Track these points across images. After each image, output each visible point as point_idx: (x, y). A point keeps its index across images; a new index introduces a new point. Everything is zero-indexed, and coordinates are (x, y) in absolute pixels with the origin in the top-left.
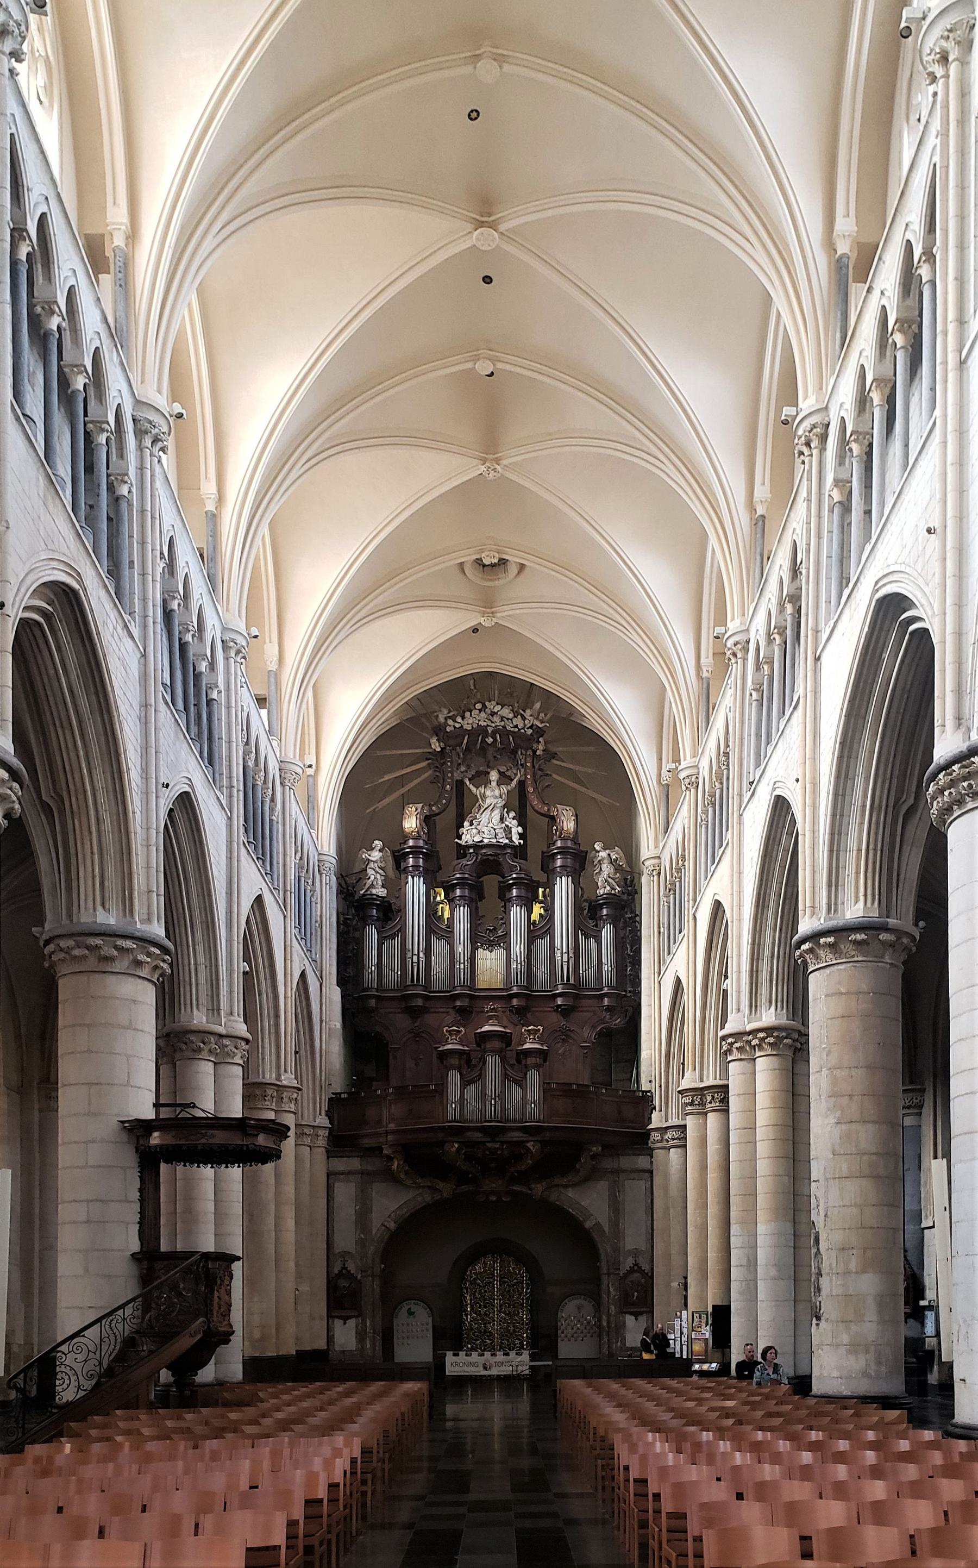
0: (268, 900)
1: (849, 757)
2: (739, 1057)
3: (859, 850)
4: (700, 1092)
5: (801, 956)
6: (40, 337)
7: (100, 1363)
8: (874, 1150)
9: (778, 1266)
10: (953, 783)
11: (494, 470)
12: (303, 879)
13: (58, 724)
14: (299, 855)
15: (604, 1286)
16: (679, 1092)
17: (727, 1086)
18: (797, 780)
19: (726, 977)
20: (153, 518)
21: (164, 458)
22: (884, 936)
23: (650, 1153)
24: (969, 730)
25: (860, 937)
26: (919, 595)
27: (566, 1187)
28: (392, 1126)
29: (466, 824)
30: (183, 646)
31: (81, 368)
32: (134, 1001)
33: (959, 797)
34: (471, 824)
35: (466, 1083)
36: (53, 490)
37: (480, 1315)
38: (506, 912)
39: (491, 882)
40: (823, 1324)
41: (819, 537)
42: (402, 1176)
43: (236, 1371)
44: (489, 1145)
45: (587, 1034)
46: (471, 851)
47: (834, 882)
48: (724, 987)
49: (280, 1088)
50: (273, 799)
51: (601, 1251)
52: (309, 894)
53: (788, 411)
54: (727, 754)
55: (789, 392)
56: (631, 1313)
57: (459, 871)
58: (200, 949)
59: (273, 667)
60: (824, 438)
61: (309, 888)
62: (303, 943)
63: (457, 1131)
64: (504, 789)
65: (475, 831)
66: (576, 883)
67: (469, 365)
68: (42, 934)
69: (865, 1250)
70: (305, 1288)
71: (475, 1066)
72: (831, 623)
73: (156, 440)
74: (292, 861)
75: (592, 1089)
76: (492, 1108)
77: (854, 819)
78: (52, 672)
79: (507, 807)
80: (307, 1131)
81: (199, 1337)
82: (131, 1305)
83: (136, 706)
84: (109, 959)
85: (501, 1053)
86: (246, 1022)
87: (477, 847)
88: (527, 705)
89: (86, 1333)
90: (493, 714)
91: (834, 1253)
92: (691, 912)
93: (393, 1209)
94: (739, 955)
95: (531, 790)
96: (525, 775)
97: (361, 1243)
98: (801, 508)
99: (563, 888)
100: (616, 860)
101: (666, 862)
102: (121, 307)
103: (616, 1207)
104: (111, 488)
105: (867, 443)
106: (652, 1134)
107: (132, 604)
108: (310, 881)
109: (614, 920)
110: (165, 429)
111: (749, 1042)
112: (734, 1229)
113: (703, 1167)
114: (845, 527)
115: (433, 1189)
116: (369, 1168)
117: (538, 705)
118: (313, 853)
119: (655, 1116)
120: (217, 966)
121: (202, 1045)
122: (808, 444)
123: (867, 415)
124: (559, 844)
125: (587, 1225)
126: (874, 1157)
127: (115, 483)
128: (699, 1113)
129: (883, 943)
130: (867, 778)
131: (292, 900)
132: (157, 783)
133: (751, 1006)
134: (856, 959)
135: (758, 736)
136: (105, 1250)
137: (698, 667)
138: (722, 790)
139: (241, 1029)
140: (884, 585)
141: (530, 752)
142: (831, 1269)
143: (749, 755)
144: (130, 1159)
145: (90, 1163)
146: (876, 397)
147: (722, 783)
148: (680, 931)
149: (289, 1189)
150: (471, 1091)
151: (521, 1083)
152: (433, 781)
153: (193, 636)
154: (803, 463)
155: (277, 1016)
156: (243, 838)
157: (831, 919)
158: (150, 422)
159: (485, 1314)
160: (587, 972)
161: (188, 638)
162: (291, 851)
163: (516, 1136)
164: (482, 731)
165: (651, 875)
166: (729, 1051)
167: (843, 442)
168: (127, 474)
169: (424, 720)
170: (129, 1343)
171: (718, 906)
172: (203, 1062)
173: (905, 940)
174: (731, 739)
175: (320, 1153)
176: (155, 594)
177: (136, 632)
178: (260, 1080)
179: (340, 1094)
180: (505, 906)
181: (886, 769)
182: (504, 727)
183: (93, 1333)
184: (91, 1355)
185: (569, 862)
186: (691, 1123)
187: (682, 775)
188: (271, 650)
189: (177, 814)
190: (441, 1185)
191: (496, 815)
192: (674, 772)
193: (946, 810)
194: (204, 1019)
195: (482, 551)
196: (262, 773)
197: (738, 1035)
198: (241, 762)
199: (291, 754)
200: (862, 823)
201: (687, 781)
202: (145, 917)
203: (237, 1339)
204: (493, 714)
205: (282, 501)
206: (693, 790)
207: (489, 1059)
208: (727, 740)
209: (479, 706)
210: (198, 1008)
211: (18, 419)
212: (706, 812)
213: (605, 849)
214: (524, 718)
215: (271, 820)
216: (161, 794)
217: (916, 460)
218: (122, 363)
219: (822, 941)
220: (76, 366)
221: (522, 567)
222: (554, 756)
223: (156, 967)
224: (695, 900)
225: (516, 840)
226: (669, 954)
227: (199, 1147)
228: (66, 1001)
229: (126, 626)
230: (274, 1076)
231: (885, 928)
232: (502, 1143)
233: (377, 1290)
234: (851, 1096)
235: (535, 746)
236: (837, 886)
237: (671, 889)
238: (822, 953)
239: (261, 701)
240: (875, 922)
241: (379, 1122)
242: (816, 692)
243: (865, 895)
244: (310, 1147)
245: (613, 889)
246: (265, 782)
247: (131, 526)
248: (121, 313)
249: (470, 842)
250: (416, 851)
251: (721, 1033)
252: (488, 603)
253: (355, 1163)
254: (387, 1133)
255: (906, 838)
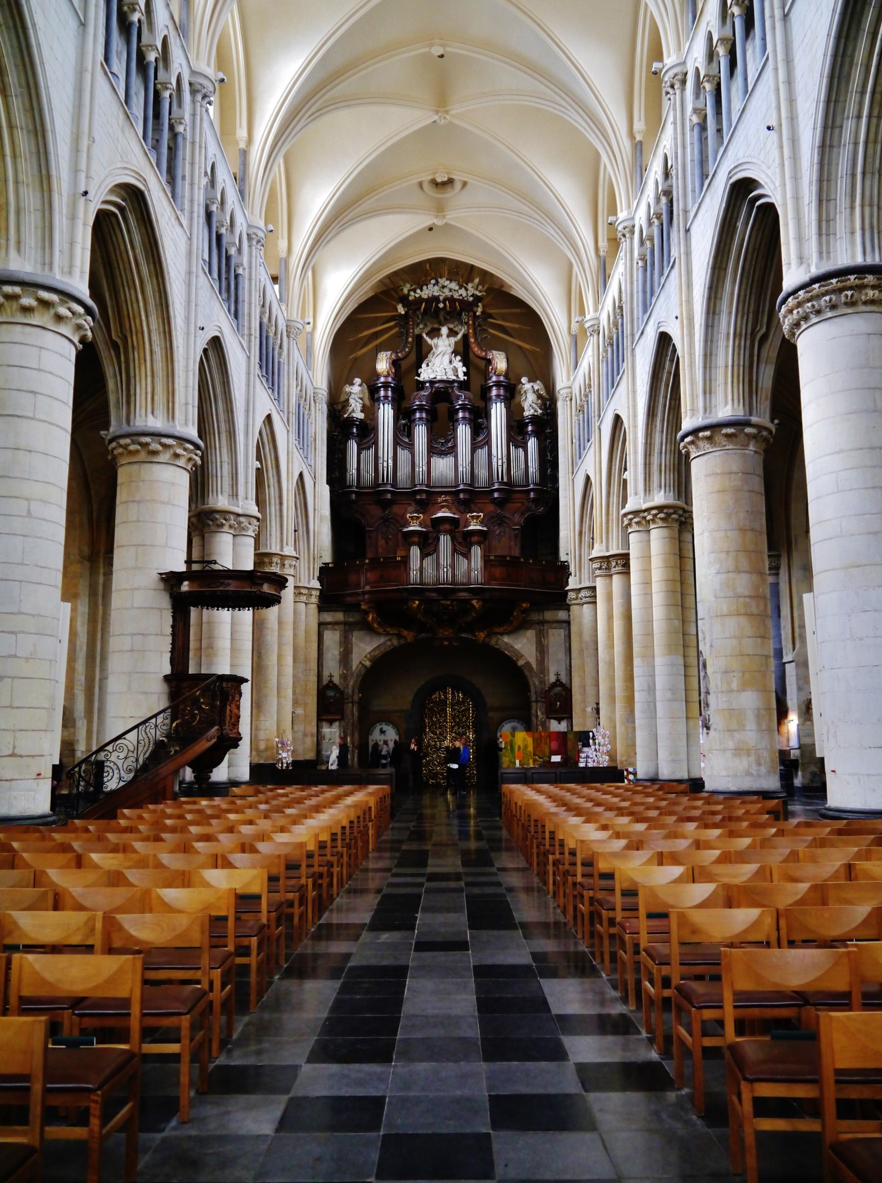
0: (276, 418)
1: (715, 298)
2: (637, 529)
3: (727, 366)
4: (607, 559)
5: (685, 447)
6: (125, 26)
7: (137, 760)
8: (747, 593)
9: (673, 690)
10: (799, 305)
11: (445, 118)
12: (302, 406)
13: (125, 284)
14: (299, 388)
15: (533, 711)
16: (590, 560)
17: (628, 555)
18: (677, 318)
19: (625, 469)
20: (200, 147)
21: (211, 109)
22: (748, 430)
23: (567, 608)
24: (809, 266)
25: (730, 430)
26: (763, 176)
27: (502, 634)
28: (367, 588)
29: (424, 365)
30: (219, 237)
31: (153, 47)
32: (173, 484)
33: (804, 315)
34: (428, 365)
35: (423, 556)
36: (129, 123)
37: (436, 734)
38: (455, 430)
39: (442, 407)
40: (711, 732)
41: (684, 147)
42: (376, 626)
43: (244, 774)
44: (443, 602)
45: (518, 520)
46: (428, 385)
47: (708, 391)
48: (625, 477)
49: (283, 557)
50: (281, 347)
51: (531, 683)
52: (306, 417)
53: (656, 66)
54: (621, 308)
55: (657, 53)
56: (555, 719)
57: (420, 399)
58: (225, 451)
59: (283, 254)
60: (684, 82)
61: (306, 412)
62: (301, 451)
63: (419, 592)
64: (453, 340)
65: (430, 371)
66: (508, 408)
67: (427, 50)
68: (106, 435)
69: (744, 673)
70: (300, 711)
71: (431, 544)
72: (697, 205)
73: (205, 96)
74: (294, 392)
75: (522, 560)
76: (445, 574)
77: (722, 343)
78: (122, 248)
79: (455, 352)
80: (304, 591)
81: (214, 740)
82: (161, 715)
83: (183, 273)
84: (155, 453)
85: (452, 533)
86: (258, 504)
87: (432, 382)
88: (469, 280)
89: (127, 736)
90: (443, 287)
91: (719, 676)
92: (597, 424)
93: (368, 651)
94: (636, 453)
95: (472, 340)
96: (468, 330)
97: (344, 677)
98: (669, 129)
99: (498, 413)
100: (538, 391)
101: (576, 391)
102: (184, 13)
103: (542, 650)
104: (172, 128)
105: (715, 82)
106: (569, 593)
107: (183, 203)
108: (307, 408)
109: (537, 434)
110: (211, 89)
111: (644, 518)
112: (637, 662)
113: (610, 617)
114: (703, 140)
115: (399, 636)
116: (351, 620)
117: (477, 281)
118: (310, 387)
119: (571, 580)
120: (236, 463)
121: (224, 522)
122: (672, 86)
123: (715, 64)
124: (494, 379)
125: (521, 663)
126: (748, 600)
127: (175, 125)
128: (606, 576)
129: (747, 435)
130: (730, 313)
131: (293, 419)
132: (195, 326)
133: (645, 490)
134: (727, 447)
135: (644, 292)
136: (143, 673)
137: (597, 249)
138: (618, 334)
139: (254, 510)
140: (736, 173)
141: (471, 314)
142: (717, 688)
143: (638, 306)
144: (165, 602)
145: (135, 605)
146: (721, 51)
147: (617, 329)
148: (589, 441)
149: (289, 634)
150: (428, 562)
151: (467, 555)
152: (400, 335)
153: (227, 229)
154: (670, 99)
155: (281, 504)
156: (258, 371)
157: (707, 418)
158: (201, 85)
159: (440, 734)
160: (517, 472)
161: (223, 231)
162: (293, 383)
163: (463, 595)
164: (436, 299)
165: (565, 400)
166: (630, 524)
167: (698, 83)
168: (183, 118)
169: (392, 292)
170: (159, 746)
171: (617, 419)
172: (225, 534)
173: (765, 433)
174: (624, 296)
175: (313, 608)
176: (200, 198)
177: (185, 222)
178: (268, 551)
179: (328, 564)
180: (453, 425)
181: (744, 307)
182: (452, 296)
183: (132, 736)
184: (130, 754)
185: (502, 392)
186: (600, 584)
187: (587, 325)
188: (283, 244)
189: (210, 353)
190: (405, 633)
191: (446, 359)
192: (581, 323)
193: (795, 325)
194: (226, 503)
195: (435, 173)
196: (274, 328)
197: (636, 513)
198: (258, 317)
199: (295, 315)
200: (727, 347)
201: (591, 329)
202: (183, 422)
203: (245, 744)
204: (443, 287)
205: (294, 140)
206: (595, 336)
207: (442, 537)
208: (620, 300)
209: (433, 282)
210: (222, 492)
211: (106, 73)
212: (606, 351)
213: (529, 381)
214: (467, 290)
215: (279, 362)
216: (198, 335)
217: (755, 85)
218: (183, 47)
219: (701, 434)
220: (151, 46)
221: (465, 184)
222: (491, 316)
223: (190, 459)
224: (599, 416)
225: (462, 377)
226: (580, 458)
227: (218, 593)
228: (122, 484)
229: (178, 218)
230: (278, 548)
231: (748, 424)
232: (453, 601)
233: (356, 713)
234: (728, 552)
235: (475, 309)
236: (710, 393)
237: (581, 410)
238: (701, 444)
239: (275, 279)
240: (740, 420)
241: (358, 586)
242: (688, 254)
243: (733, 400)
244: (306, 604)
245: (536, 411)
246: (276, 334)
247: (185, 152)
248: (184, 16)
249: (427, 379)
250: (386, 386)
251: (623, 512)
252: (440, 209)
253: (340, 616)
254: (364, 593)
255: (761, 359)
